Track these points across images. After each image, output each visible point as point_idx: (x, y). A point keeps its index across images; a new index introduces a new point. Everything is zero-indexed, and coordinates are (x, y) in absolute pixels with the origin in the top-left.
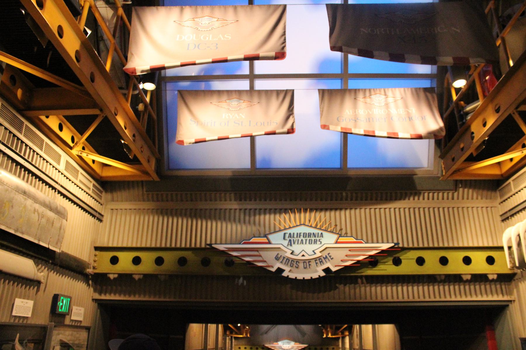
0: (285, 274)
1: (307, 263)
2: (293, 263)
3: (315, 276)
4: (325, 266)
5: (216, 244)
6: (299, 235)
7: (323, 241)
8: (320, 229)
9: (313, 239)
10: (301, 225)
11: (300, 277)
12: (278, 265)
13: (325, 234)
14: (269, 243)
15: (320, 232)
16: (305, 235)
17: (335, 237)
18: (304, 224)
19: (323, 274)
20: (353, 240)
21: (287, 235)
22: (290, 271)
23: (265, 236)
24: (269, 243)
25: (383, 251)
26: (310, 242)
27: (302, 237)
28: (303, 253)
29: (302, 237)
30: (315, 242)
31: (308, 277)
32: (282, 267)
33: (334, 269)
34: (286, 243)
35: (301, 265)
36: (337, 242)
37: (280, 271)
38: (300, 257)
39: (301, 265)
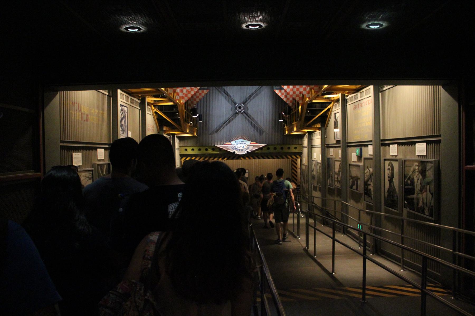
0: (236, 153)
1: (242, 150)
2: (238, 150)
3: (244, 153)
4: (247, 151)
5: (216, 145)
6: (239, 142)
7: (246, 143)
8: (246, 140)
9: (244, 143)
10: (240, 138)
11: (240, 154)
12: (234, 151)
13: (247, 141)
14: (231, 144)
15: (246, 141)
16: (241, 142)
17: (250, 142)
18: (241, 139)
19: (246, 153)
20: (255, 143)
21: (236, 142)
22: (237, 152)
23: (230, 142)
24: (231, 144)
25: (263, 146)
26: (243, 144)
27: (240, 142)
28: (241, 147)
29: (240, 142)
30: (244, 144)
31: (242, 154)
32: (235, 151)
33: (249, 152)
34: (236, 144)
35: (240, 150)
36: (250, 144)
37: (234, 152)
38: (240, 148)
39: (240, 150)
